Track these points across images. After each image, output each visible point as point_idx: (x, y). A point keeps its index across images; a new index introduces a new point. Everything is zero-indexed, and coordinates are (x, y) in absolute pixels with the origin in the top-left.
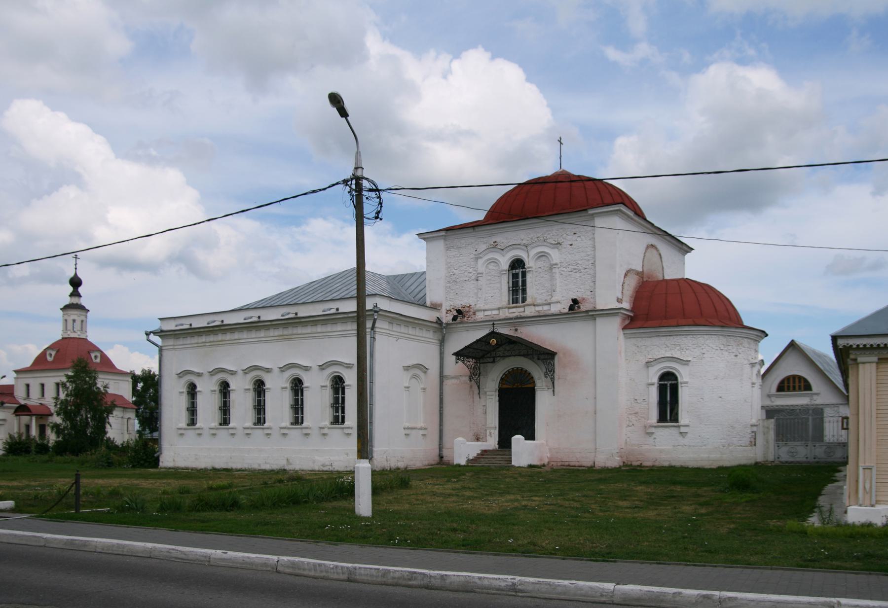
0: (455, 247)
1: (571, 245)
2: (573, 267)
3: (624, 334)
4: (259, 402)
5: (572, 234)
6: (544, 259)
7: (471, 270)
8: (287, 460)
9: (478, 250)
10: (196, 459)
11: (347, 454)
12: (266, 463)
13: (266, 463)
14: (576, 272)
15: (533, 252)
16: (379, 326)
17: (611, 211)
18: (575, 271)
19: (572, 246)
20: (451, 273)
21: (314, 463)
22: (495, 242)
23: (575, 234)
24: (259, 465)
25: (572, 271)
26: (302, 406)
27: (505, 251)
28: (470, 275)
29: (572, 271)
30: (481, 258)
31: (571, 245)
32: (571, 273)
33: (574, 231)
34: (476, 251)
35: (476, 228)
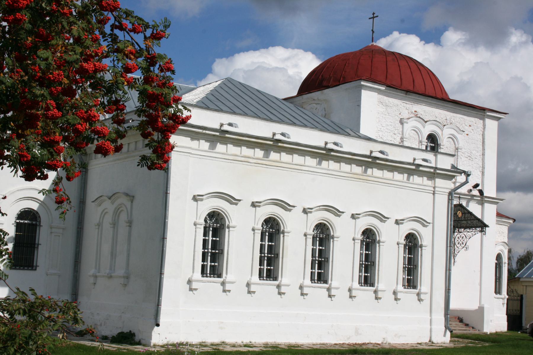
0: (384, 104)
1: (467, 135)
2: (469, 155)
3: (497, 220)
5: (468, 125)
9: (401, 114)
14: (470, 159)
18: (469, 158)
19: (468, 136)
20: (379, 129)
23: (470, 126)
25: (467, 158)
27: (427, 123)
28: (395, 136)
29: (467, 158)
30: (407, 123)
34: (400, 114)
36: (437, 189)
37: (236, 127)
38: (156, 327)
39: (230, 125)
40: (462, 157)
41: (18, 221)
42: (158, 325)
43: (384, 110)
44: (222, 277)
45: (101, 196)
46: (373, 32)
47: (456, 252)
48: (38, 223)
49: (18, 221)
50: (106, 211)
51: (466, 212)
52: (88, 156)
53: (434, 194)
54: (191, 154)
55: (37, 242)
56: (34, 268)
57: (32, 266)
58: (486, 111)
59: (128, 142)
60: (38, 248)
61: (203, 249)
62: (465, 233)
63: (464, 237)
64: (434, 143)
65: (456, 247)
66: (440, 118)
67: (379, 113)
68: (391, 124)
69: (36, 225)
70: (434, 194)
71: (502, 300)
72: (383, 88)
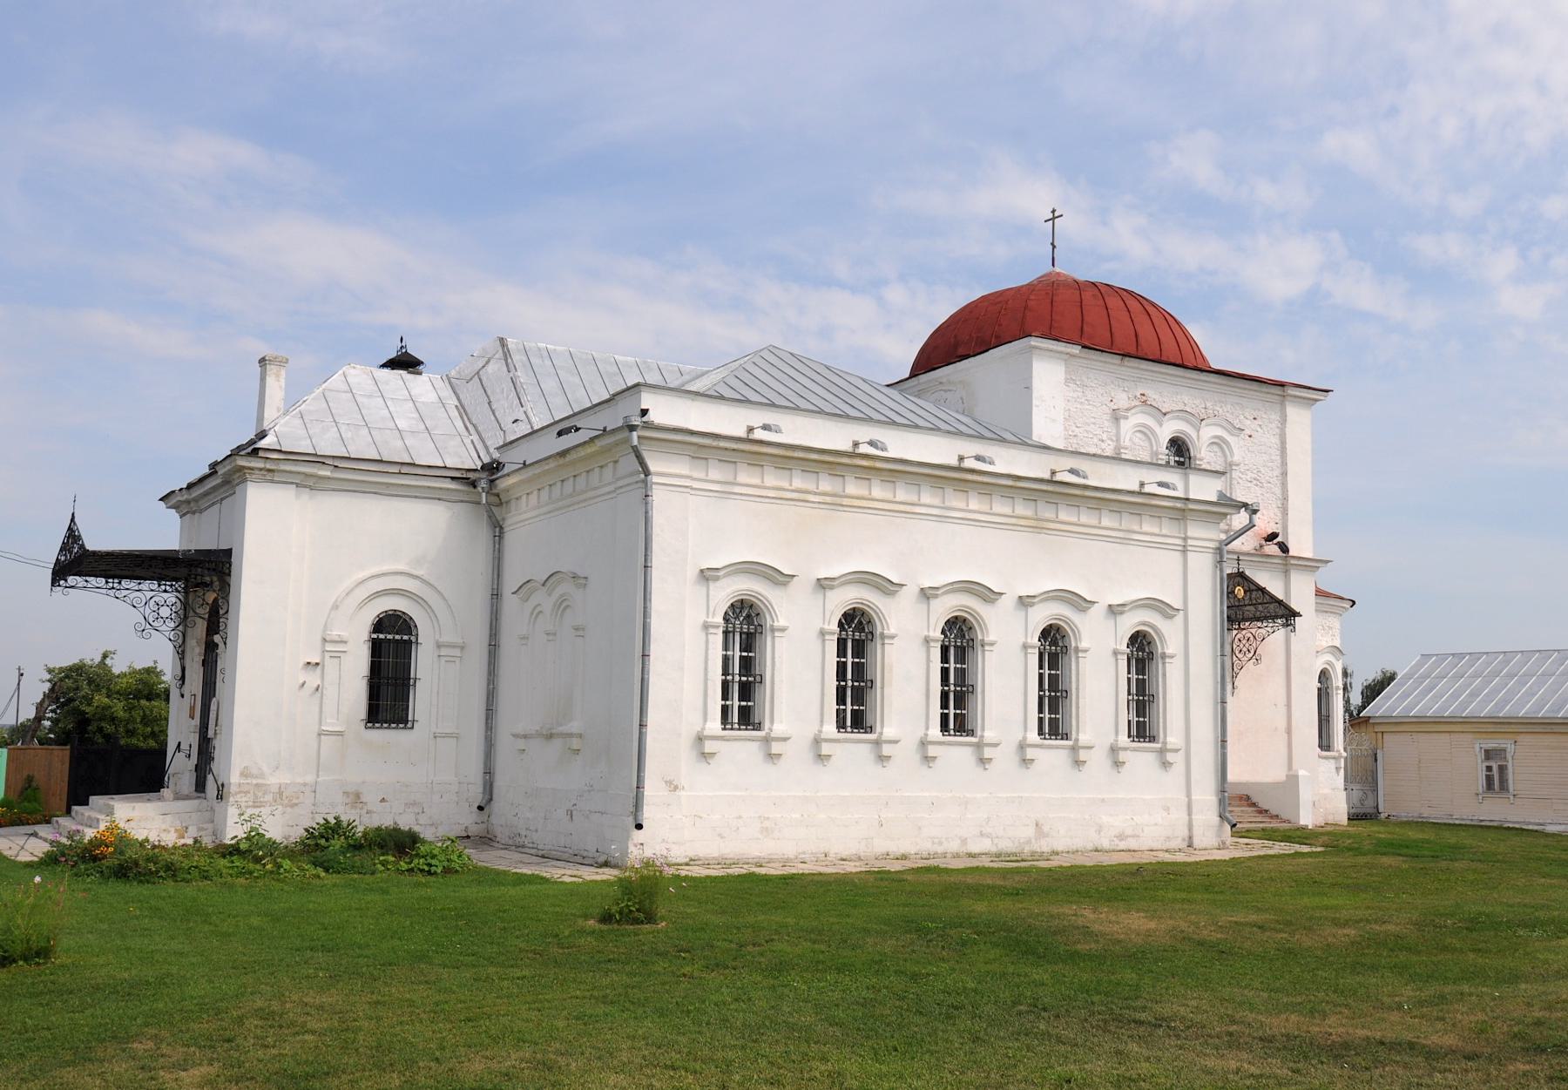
0: (1078, 383)
1: (1250, 436)
2: (1254, 476)
3: (1316, 603)
4: (1141, 685)
5: (1252, 418)
6: (1215, 450)
7: (1105, 437)
8: (1037, 825)
10: (765, 830)
11: (1167, 809)
12: (982, 834)
13: (982, 834)
14: (1257, 485)
15: (1209, 432)
16: (1196, 535)
17: (1304, 398)
18: (1255, 482)
20: (1070, 433)
21: (1100, 832)
22: (1144, 395)
23: (1255, 419)
24: (964, 841)
25: (1251, 482)
26: (1041, 693)
27: (1167, 417)
29: (1251, 482)
30: (1126, 418)
31: (1250, 436)
32: (1249, 485)
33: (1255, 414)
35: (1127, 359)
36: (1190, 542)
37: (778, 431)
38: (637, 833)
39: (766, 427)
40: (1240, 481)
41: (375, 636)
42: (639, 827)
43: (1080, 394)
44: (764, 730)
45: (528, 582)
46: (1054, 247)
47: (1235, 669)
48: (413, 639)
49: (375, 636)
50: (539, 609)
51: (1253, 587)
52: (504, 505)
53: (1184, 551)
54: (692, 489)
55: (412, 676)
56: (409, 725)
57: (406, 722)
58: (1286, 388)
59: (574, 474)
60: (415, 685)
61: (723, 675)
62: (1253, 631)
63: (1252, 638)
64: (1182, 456)
65: (1235, 658)
66: (1194, 406)
67: (1068, 401)
68: (1093, 420)
69: (410, 642)
70: (1184, 551)
71: (1333, 761)
72: (1076, 350)
